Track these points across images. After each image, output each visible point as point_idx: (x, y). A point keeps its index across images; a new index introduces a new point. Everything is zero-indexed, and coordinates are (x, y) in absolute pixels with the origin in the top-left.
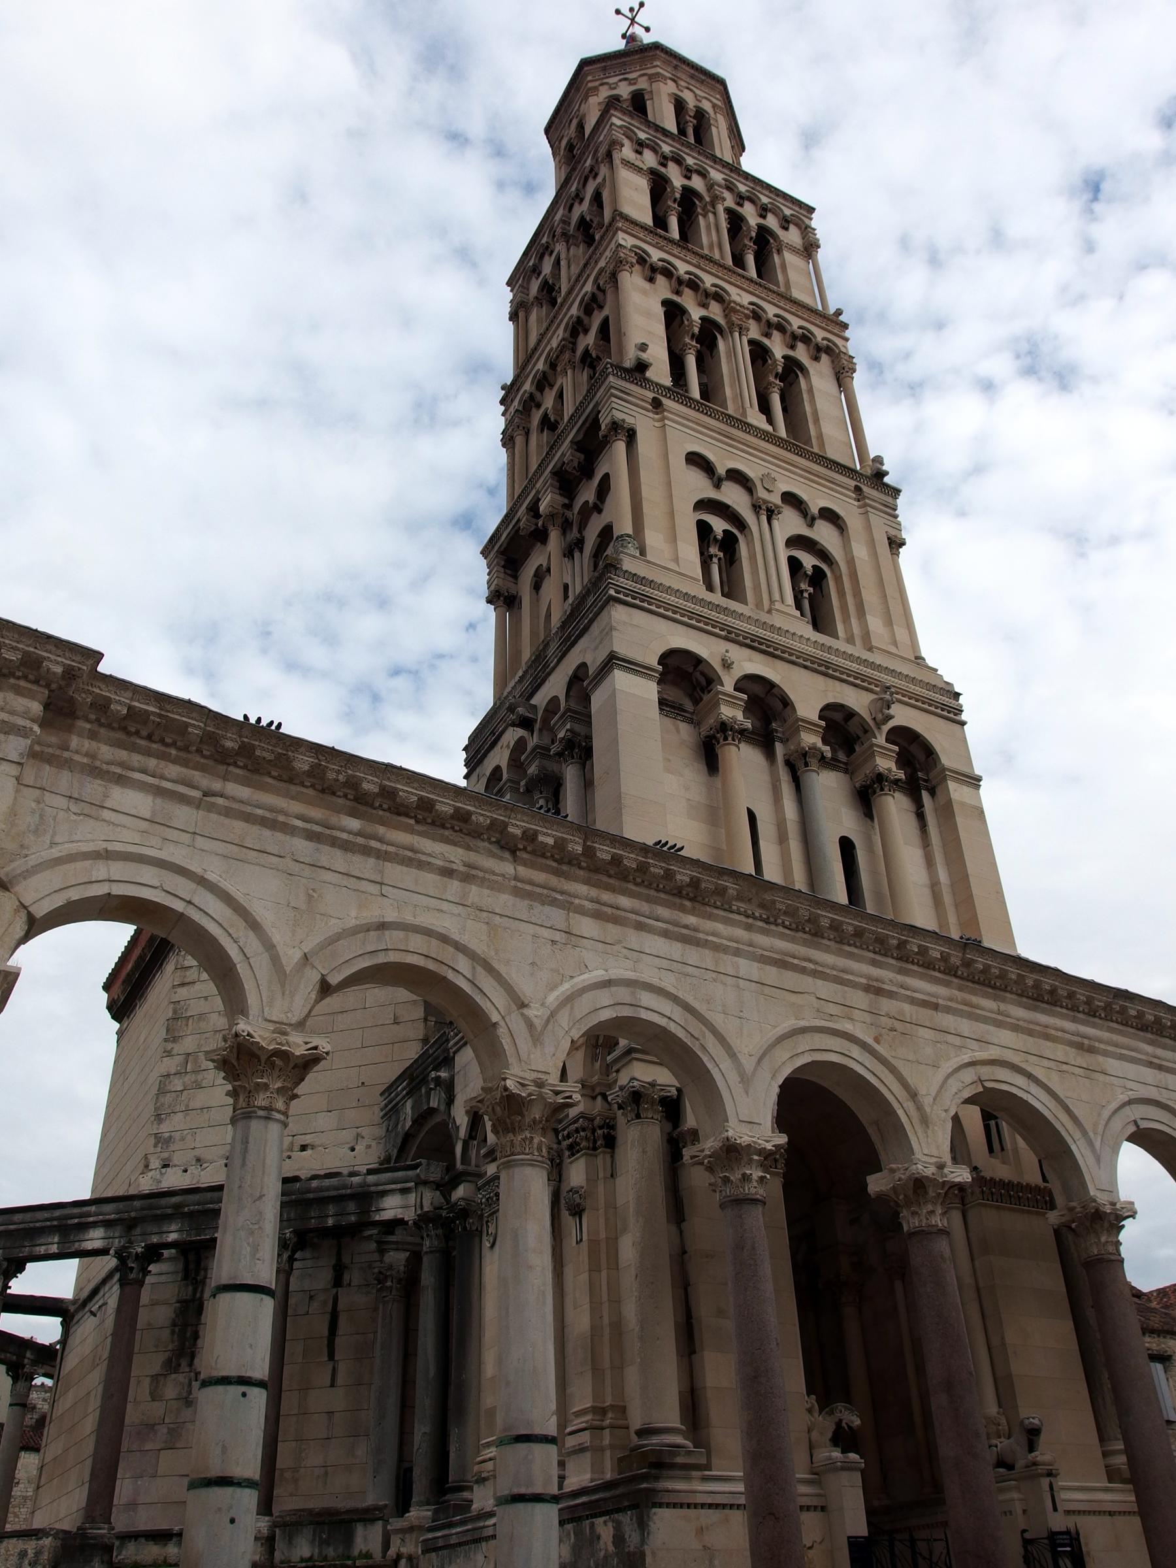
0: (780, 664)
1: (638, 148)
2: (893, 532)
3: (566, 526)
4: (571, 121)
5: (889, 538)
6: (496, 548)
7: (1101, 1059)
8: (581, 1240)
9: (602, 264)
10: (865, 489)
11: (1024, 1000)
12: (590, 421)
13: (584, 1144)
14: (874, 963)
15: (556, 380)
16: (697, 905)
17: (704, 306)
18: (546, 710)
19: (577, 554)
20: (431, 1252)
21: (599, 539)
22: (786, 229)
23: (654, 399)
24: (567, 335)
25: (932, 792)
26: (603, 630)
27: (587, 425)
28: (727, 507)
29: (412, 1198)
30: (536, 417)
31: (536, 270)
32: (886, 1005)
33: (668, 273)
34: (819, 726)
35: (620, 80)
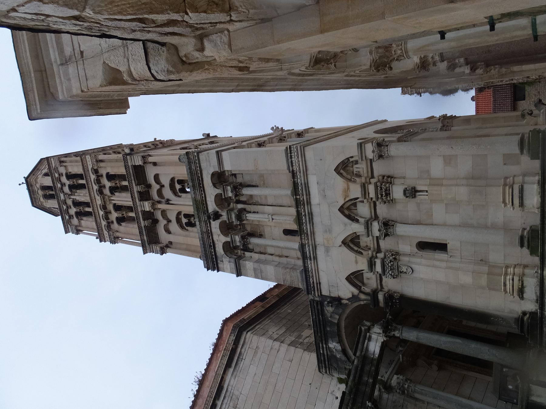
3: (159, 202)
4: (38, 193)
6: (147, 245)
8: (427, 191)
9: (90, 167)
12: (135, 174)
13: (387, 185)
15: (111, 211)
18: (217, 206)
19: (171, 202)
20: (402, 330)
21: (172, 191)
24: (100, 195)
26: (206, 159)
27: (135, 176)
29: (374, 336)
30: (115, 226)
31: (71, 217)
35: (41, 172)
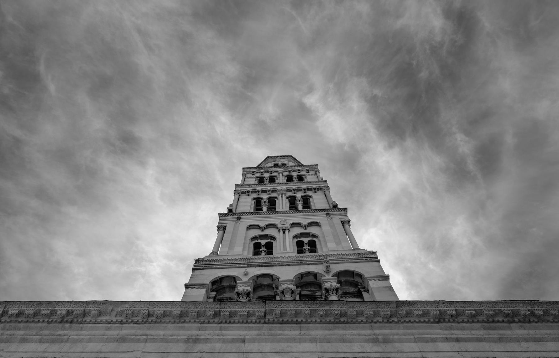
0: (274, 268)
1: (253, 174)
2: (343, 220)
5: (342, 222)
7: (397, 345)
10: (330, 213)
11: (325, 325)
14: (200, 329)
16: (73, 325)
17: (269, 195)
22: (308, 172)
23: (237, 218)
25: (368, 291)
28: (267, 235)
32: (200, 347)
33: (255, 192)
34: (292, 281)
